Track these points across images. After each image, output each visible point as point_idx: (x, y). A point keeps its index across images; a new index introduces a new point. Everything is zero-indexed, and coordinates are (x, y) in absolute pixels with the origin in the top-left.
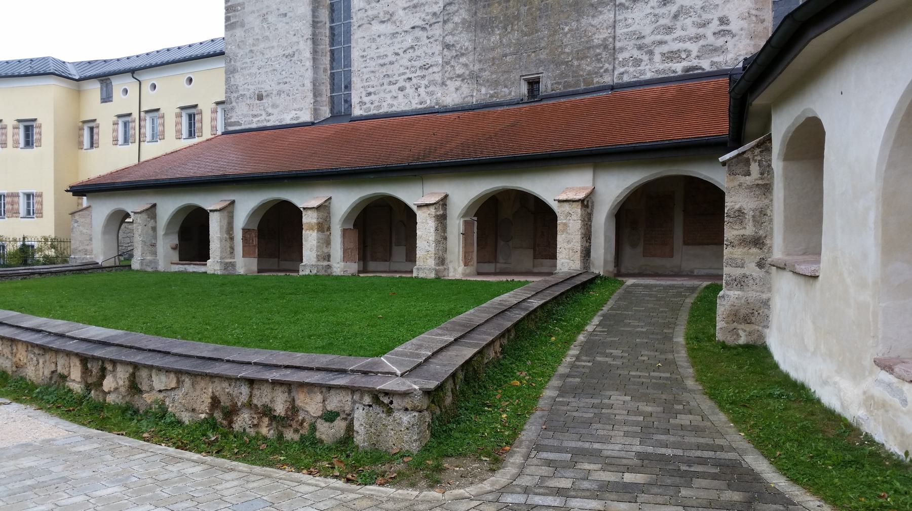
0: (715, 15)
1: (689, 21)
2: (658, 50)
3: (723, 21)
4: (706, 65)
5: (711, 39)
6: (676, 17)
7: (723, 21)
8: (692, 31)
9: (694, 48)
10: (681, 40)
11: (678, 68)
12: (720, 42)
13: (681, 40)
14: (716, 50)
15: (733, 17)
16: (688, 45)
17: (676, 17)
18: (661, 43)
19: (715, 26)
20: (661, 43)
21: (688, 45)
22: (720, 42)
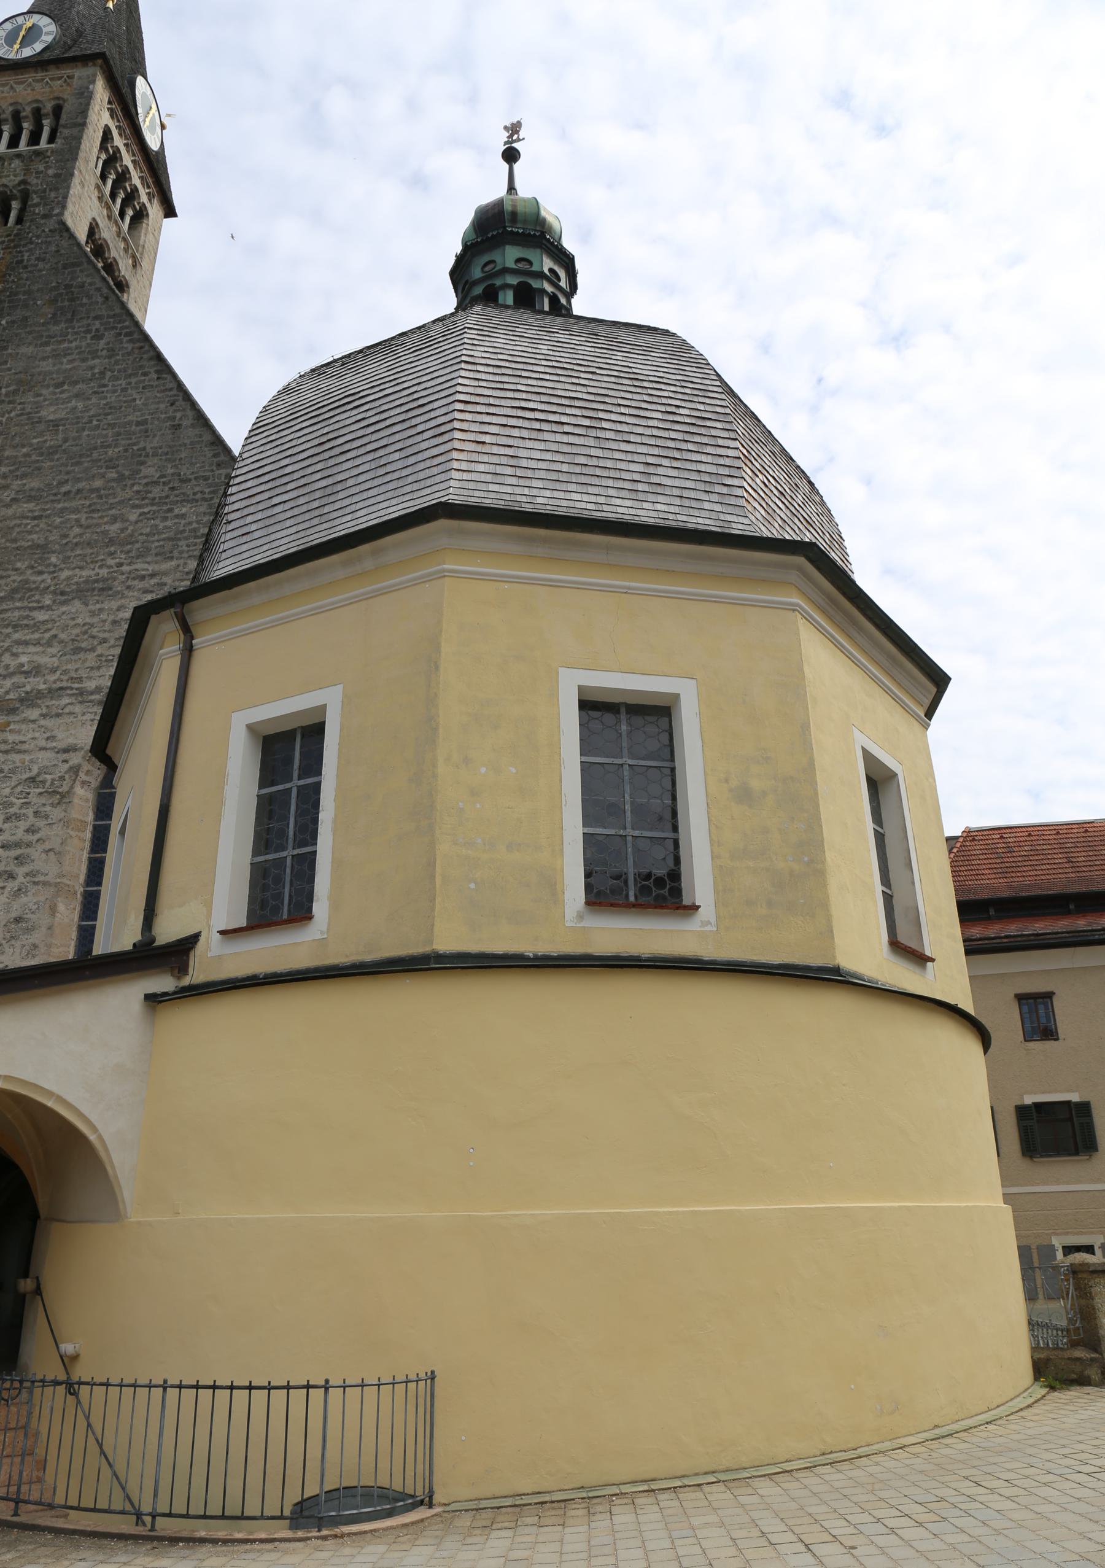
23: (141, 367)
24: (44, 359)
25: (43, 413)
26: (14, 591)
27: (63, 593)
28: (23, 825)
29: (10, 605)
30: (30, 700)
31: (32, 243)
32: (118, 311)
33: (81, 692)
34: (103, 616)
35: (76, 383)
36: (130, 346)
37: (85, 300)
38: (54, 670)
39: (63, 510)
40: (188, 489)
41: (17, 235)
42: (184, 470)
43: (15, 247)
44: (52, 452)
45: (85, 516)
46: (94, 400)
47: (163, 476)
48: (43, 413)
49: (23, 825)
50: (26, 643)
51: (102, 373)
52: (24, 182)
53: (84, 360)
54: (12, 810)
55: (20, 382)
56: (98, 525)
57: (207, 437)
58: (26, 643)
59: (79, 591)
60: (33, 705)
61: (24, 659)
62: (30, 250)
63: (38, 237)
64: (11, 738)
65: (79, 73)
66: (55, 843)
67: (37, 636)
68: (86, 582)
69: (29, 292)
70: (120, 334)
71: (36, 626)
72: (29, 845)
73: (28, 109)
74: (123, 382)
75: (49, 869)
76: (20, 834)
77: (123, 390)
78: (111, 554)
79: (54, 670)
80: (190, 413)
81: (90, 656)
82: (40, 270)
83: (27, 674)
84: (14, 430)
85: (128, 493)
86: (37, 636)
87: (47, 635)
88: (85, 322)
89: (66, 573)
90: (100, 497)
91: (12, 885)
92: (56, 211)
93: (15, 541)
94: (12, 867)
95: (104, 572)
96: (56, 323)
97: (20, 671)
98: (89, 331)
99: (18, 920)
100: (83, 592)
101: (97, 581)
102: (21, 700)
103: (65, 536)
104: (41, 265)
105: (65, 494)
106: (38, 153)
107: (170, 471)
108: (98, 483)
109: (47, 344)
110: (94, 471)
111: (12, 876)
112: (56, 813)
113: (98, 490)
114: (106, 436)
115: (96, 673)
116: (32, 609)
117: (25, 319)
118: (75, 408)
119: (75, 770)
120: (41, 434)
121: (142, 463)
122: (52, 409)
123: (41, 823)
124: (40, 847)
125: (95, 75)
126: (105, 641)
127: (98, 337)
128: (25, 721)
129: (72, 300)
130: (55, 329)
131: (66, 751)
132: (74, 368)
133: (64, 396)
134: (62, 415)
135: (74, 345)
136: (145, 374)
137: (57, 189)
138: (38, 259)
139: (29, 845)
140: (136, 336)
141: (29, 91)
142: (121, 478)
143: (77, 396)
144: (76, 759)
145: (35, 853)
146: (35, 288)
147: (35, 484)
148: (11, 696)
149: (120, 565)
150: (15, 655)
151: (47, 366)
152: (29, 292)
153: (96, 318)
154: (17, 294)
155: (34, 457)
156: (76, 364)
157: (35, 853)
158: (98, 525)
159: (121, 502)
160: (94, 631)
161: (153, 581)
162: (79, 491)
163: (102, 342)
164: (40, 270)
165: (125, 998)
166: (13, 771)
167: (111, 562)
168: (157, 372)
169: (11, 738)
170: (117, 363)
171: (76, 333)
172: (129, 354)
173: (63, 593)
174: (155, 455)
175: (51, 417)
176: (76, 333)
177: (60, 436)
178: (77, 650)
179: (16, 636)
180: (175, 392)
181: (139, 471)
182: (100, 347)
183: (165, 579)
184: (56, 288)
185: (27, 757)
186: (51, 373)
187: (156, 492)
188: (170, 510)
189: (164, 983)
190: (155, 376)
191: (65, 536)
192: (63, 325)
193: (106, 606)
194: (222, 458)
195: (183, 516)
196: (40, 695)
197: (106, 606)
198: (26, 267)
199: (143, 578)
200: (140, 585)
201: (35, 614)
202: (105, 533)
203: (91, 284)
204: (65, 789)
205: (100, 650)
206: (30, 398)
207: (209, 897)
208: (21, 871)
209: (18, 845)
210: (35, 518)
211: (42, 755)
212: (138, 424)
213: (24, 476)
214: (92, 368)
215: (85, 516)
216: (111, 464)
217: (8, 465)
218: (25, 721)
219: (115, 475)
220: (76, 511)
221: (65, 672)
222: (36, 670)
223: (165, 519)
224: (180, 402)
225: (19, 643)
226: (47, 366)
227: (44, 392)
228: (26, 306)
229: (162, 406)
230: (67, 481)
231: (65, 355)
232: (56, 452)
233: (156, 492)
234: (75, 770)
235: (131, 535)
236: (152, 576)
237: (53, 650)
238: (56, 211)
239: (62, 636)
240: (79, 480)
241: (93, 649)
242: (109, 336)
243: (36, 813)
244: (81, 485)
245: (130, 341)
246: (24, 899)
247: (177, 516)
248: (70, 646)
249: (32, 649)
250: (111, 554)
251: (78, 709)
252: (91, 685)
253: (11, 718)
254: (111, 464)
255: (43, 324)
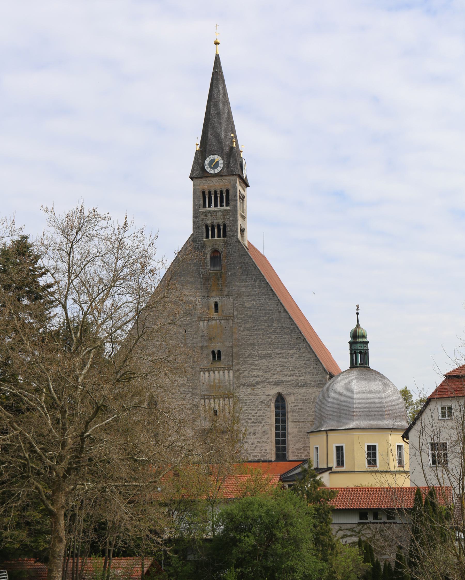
0: (264, 448)
1: (258, 449)
2: (251, 454)
3: (266, 450)
4: (262, 459)
5: (263, 453)
6: (255, 448)
7: (266, 450)
8: (259, 451)
9: (260, 455)
10: (257, 453)
11: (256, 459)
12: (265, 454)
13: (257, 453)
14: (264, 456)
15: (268, 449)
16: (258, 454)
17: (255, 448)
18: (252, 453)
19: (264, 451)
20: (252, 453)
21: (258, 454)
22: (265, 454)
23: (268, 292)
24: (242, 287)
25: (246, 305)
26: (249, 355)
27: (260, 357)
28: (262, 412)
29: (248, 359)
30: (258, 383)
31: (231, 246)
32: (259, 273)
33: (269, 382)
34: (271, 363)
35: (252, 296)
36: (264, 285)
37: (249, 268)
38: (262, 376)
39: (256, 334)
40: (285, 330)
41: (226, 242)
42: (283, 325)
43: (227, 246)
44: (250, 317)
45: (262, 336)
46: (258, 302)
47: (279, 326)
48: (246, 305)
49: (262, 412)
50: (254, 369)
51: (258, 293)
52: (224, 221)
53: (253, 289)
54: (259, 408)
55: (238, 294)
56: (265, 339)
57: (288, 316)
58: (254, 369)
59: (264, 356)
60: (259, 385)
61: (255, 373)
62: (231, 248)
63: (232, 244)
64: (255, 392)
65: (232, 178)
66: (269, 416)
67: (256, 367)
68: (265, 354)
69: (234, 264)
70: (260, 281)
71: (256, 365)
72: (264, 416)
73: (219, 191)
74: (264, 297)
75: (269, 421)
76: (261, 414)
77: (265, 299)
78: (270, 347)
79: (262, 376)
80: (282, 308)
81: (270, 373)
82: (235, 256)
83: (256, 377)
84: (239, 309)
85: (271, 331)
86: (256, 367)
87: (259, 367)
88: (251, 276)
89: (260, 352)
90: (264, 331)
91: (262, 425)
92: (235, 234)
93: (246, 342)
94: (261, 421)
95: (269, 352)
96: (243, 276)
97: (254, 376)
98: (252, 279)
99: (264, 432)
100: (266, 356)
101: (268, 354)
102: (256, 383)
103: (258, 341)
104: (235, 254)
105: (256, 329)
106: (225, 210)
107: (280, 325)
108: (263, 327)
109: (242, 282)
110: (262, 323)
111: (261, 423)
112: (268, 409)
113: (263, 329)
114: (263, 313)
115: (271, 378)
116: (254, 361)
117: (235, 273)
118: (253, 304)
119: (271, 400)
120: (246, 311)
121: (273, 322)
122: (248, 303)
123: (265, 412)
124: (266, 417)
125: (237, 180)
126: (272, 370)
127: (255, 281)
128: (258, 388)
129: (246, 268)
130: (244, 277)
131: (268, 395)
132: (251, 291)
133: (250, 299)
134: (250, 305)
135: (249, 283)
136: (269, 295)
137: (234, 226)
138: (234, 252)
139: (264, 416)
140: (265, 282)
141: (218, 184)
142: (268, 326)
143: (253, 300)
144: (270, 397)
145: (265, 418)
146: (235, 262)
147: (248, 326)
148: (253, 382)
149: (272, 350)
150: (252, 372)
151: (243, 289)
152: (234, 264)
153: (254, 275)
154: (231, 264)
155: (246, 318)
156: (251, 290)
157: (265, 418)
158: (265, 339)
159: (270, 333)
160: (269, 367)
161: (281, 355)
162: (259, 329)
163: (257, 283)
164: (235, 256)
165: (327, 473)
166: (257, 400)
167: (270, 349)
168: (272, 294)
169: (255, 392)
170: (261, 290)
171: (249, 279)
172: (264, 288)
173: (260, 357)
174: (276, 320)
175: (248, 306)
176: (249, 279)
177: (251, 312)
178: (266, 372)
179: (252, 367)
180: (278, 301)
181: (273, 325)
182: (257, 285)
183: (284, 355)
184: (241, 263)
185: (260, 397)
186: (244, 292)
187: (278, 331)
188: (282, 336)
189: (330, 471)
190: (272, 296)
191: (258, 341)
192: (245, 276)
193: (271, 361)
194: (292, 323)
195: (285, 338)
196: (260, 382)
197: (271, 361)
198: (231, 255)
199: (278, 354)
200: (278, 356)
201: (255, 362)
202: (267, 341)
203: (250, 263)
204: (269, 404)
205: (272, 372)
206: (241, 299)
207: (333, 463)
208: (263, 422)
209: (261, 416)
210: (250, 336)
211: (263, 396)
212: (271, 310)
213: (244, 323)
214: (255, 291)
215: (262, 336)
216: (265, 321)
217: (240, 320)
218: (258, 388)
219: (267, 325)
220: (259, 335)
221: (264, 377)
222: (258, 376)
223: (281, 339)
224: (279, 305)
225: (253, 369)
226: (243, 289)
227: (245, 298)
228: (234, 269)
229: (275, 305)
230: (255, 326)
231: (248, 286)
232: (251, 317)
233: (278, 331)
234: (271, 400)
235: (274, 342)
236: (280, 354)
237: (261, 371)
238: (235, 234)
239: (262, 368)
240: (258, 326)
241: (270, 372)
242: (258, 281)
243: (264, 409)
244: (259, 327)
245: (264, 283)
246: (265, 428)
247: (284, 338)
248: (265, 371)
249: (256, 371)
250: (270, 347)
251: (269, 386)
252: (271, 380)
253: (255, 387)
254: (265, 321)
255: (240, 276)
